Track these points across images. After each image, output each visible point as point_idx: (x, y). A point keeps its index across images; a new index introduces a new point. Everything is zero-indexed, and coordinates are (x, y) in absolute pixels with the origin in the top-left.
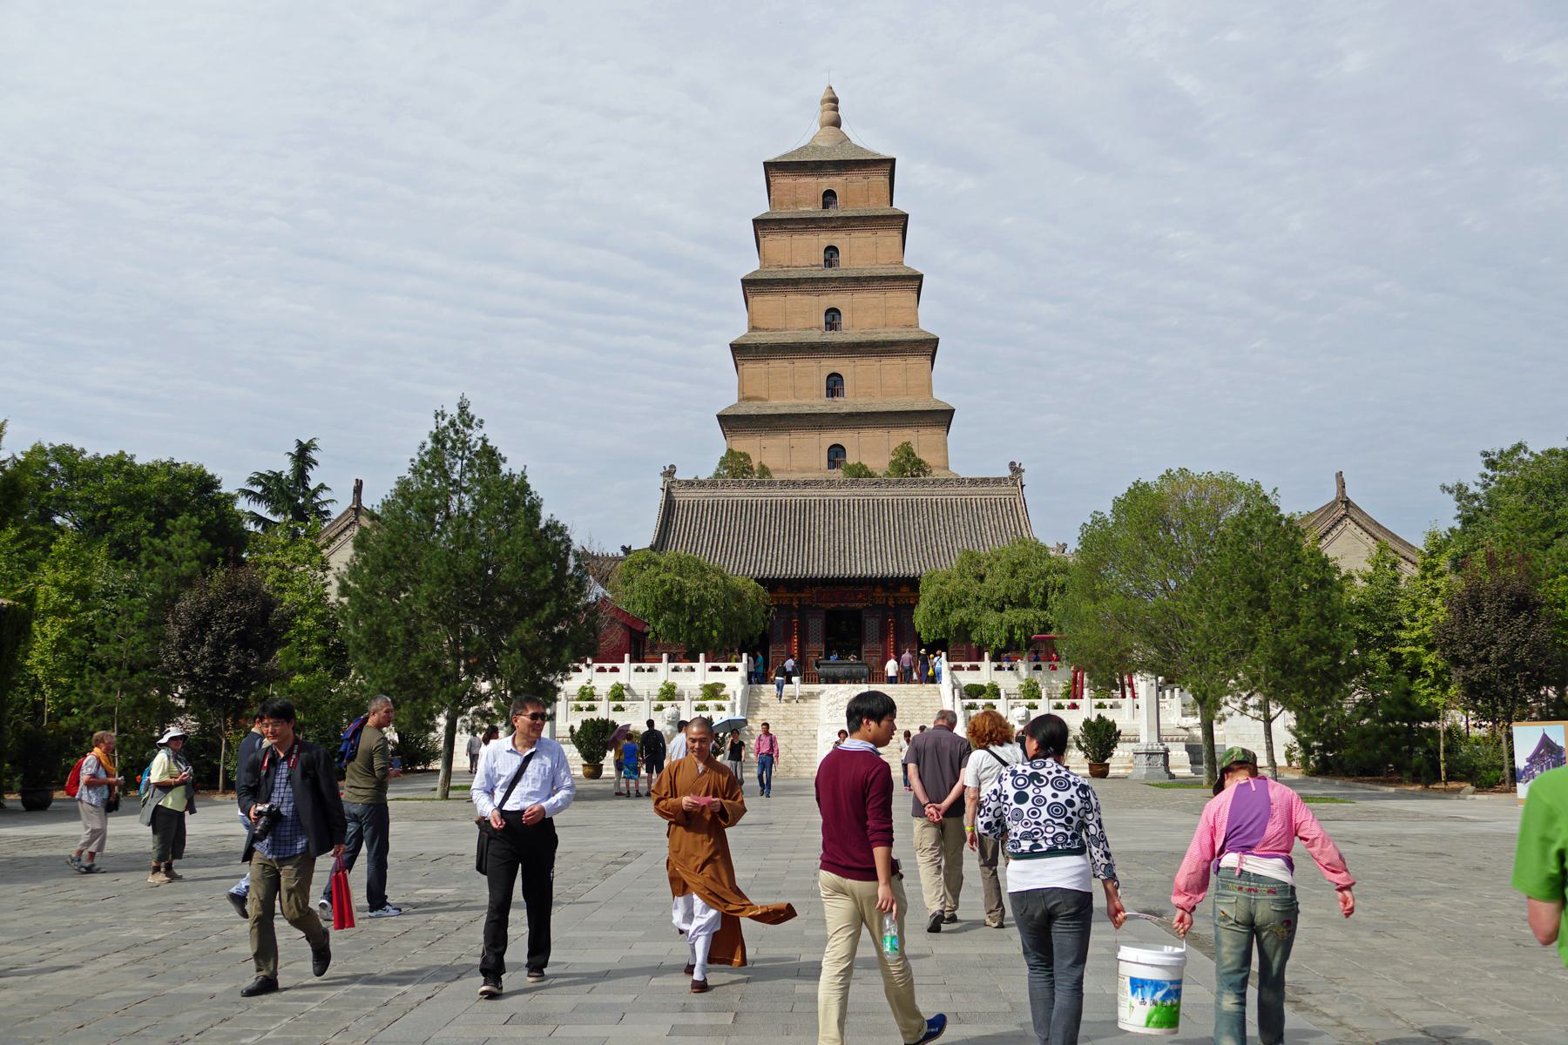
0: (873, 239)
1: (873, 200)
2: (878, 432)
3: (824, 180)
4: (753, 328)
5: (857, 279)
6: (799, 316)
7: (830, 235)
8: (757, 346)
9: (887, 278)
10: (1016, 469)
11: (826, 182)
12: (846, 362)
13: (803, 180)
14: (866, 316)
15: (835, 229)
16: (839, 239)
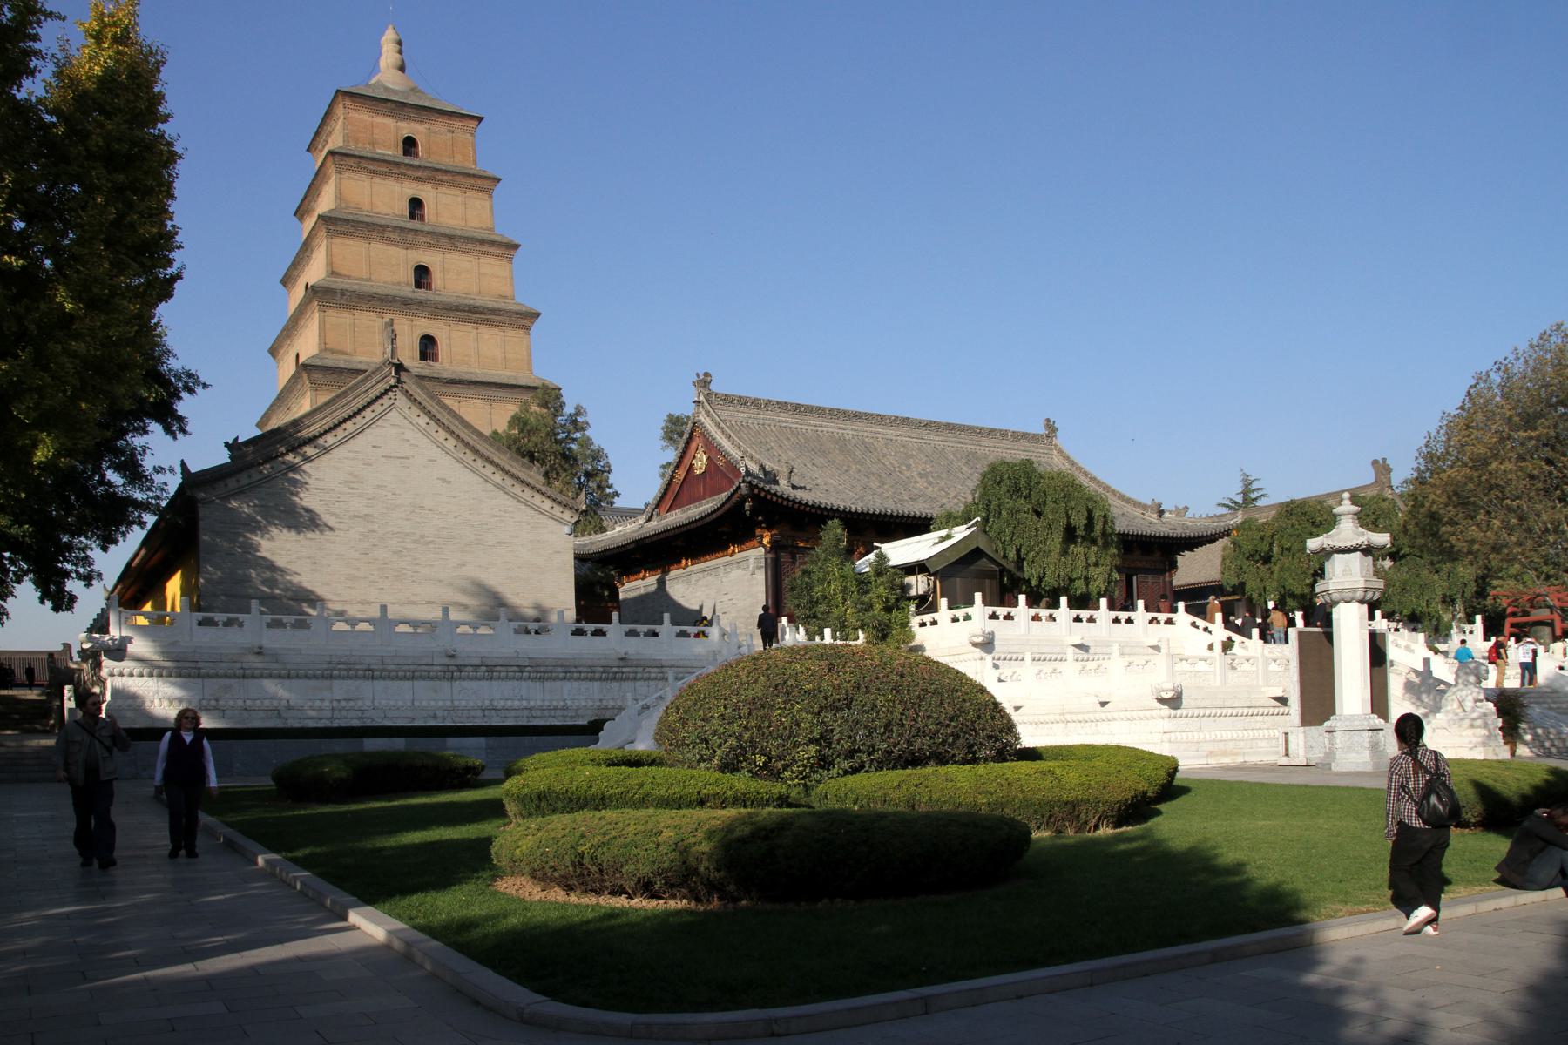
0: (460, 199)
1: (458, 158)
2: (480, 404)
3: (402, 124)
4: (333, 273)
5: (451, 237)
6: (389, 266)
7: (414, 184)
8: (343, 292)
9: (482, 242)
10: (1051, 427)
11: (407, 128)
12: (441, 324)
13: (380, 120)
14: (457, 276)
15: (419, 179)
16: (426, 192)
